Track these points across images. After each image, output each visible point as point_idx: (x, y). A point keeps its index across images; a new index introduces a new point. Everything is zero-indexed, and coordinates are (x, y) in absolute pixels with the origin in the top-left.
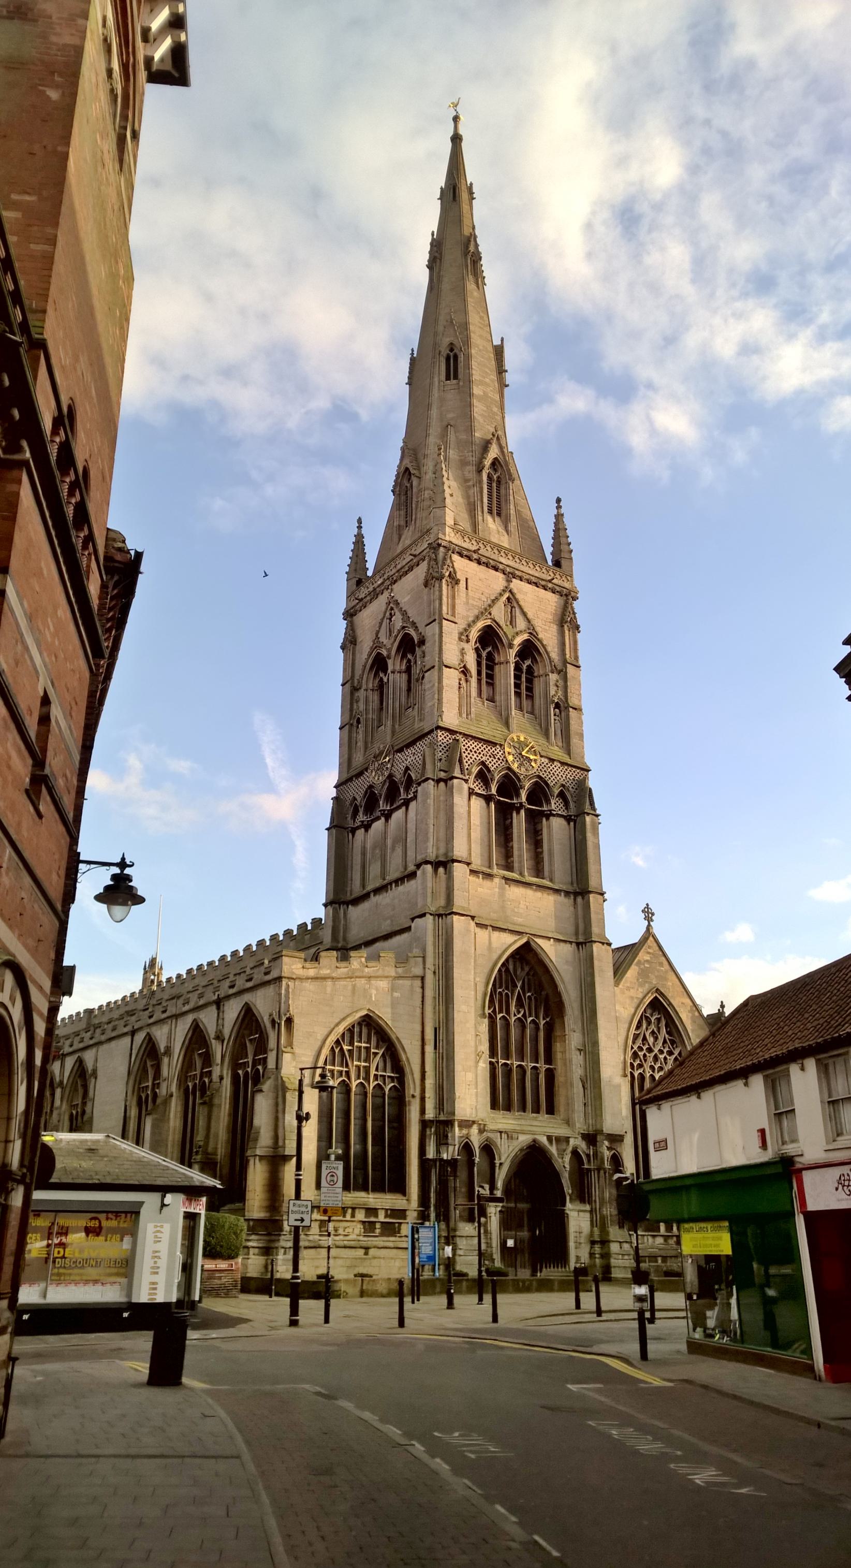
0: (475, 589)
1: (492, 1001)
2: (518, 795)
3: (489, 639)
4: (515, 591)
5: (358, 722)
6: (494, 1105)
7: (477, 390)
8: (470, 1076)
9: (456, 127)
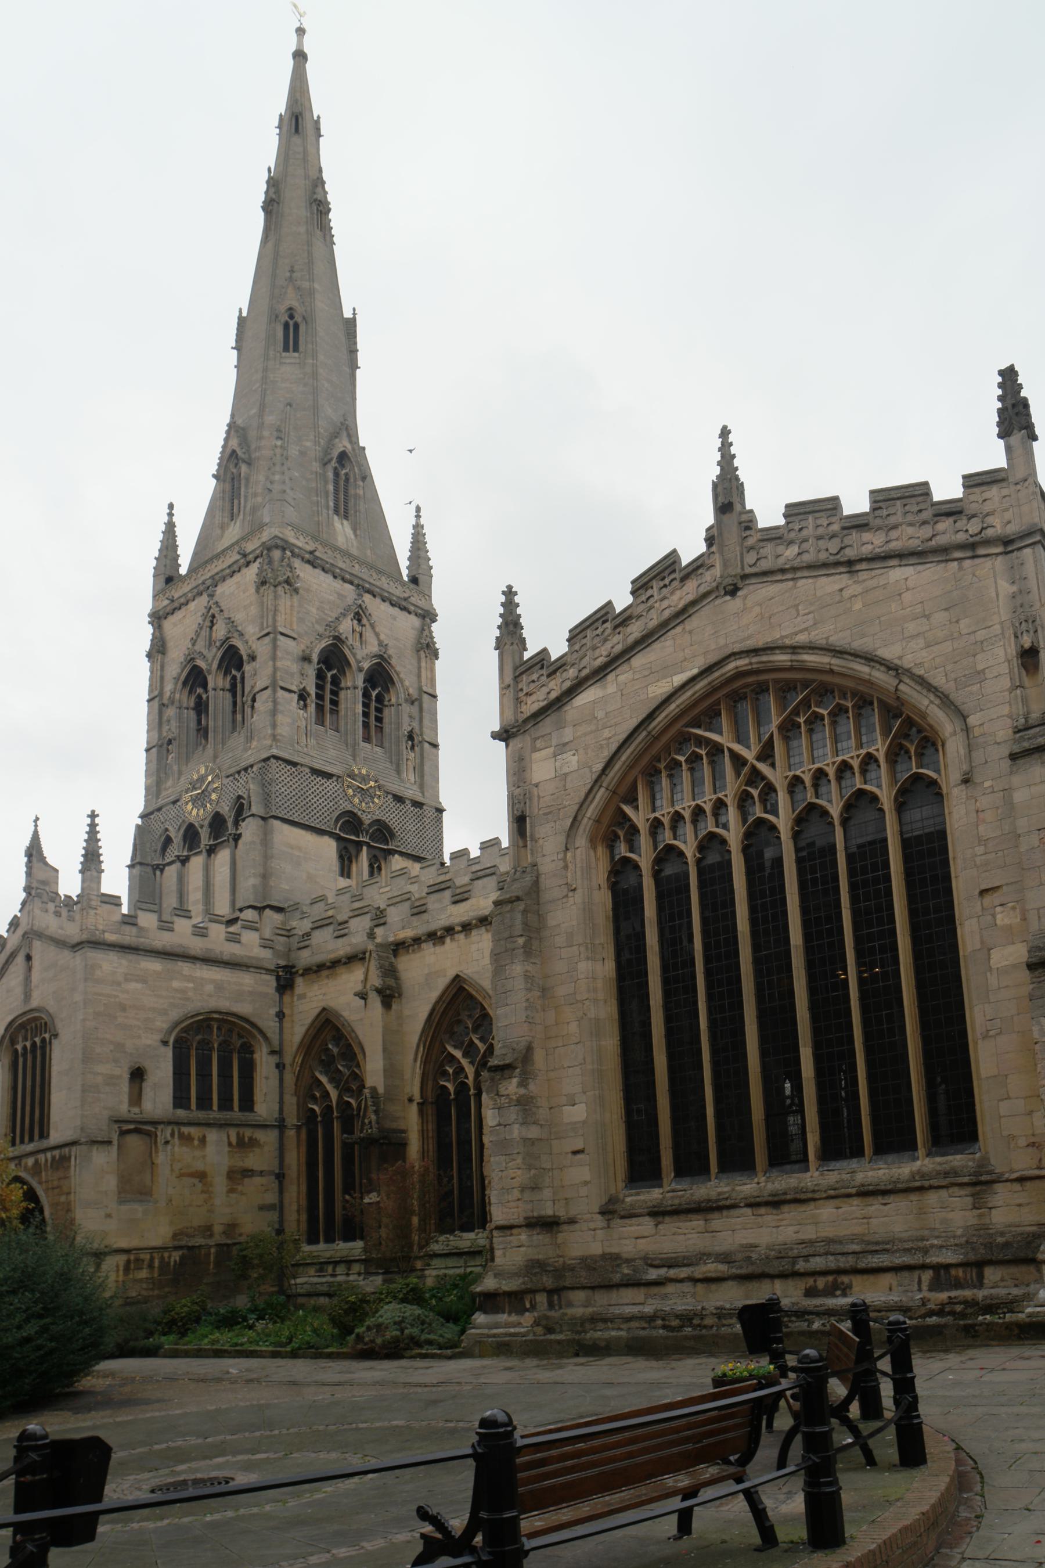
9: (300, 42)
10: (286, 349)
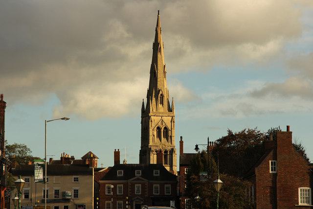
0: (155, 121)
3: (159, 129)
7: (158, 80)
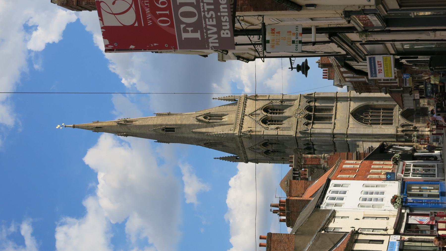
1: (367, 124)
2: (311, 115)
4: (249, 113)
5: (283, 158)
6: (392, 124)
7: (179, 122)
8: (386, 130)
10: (174, 131)
